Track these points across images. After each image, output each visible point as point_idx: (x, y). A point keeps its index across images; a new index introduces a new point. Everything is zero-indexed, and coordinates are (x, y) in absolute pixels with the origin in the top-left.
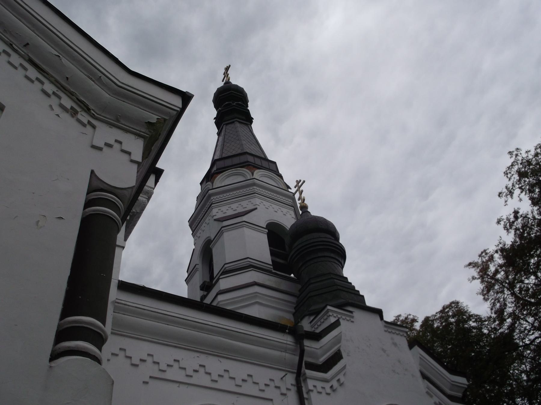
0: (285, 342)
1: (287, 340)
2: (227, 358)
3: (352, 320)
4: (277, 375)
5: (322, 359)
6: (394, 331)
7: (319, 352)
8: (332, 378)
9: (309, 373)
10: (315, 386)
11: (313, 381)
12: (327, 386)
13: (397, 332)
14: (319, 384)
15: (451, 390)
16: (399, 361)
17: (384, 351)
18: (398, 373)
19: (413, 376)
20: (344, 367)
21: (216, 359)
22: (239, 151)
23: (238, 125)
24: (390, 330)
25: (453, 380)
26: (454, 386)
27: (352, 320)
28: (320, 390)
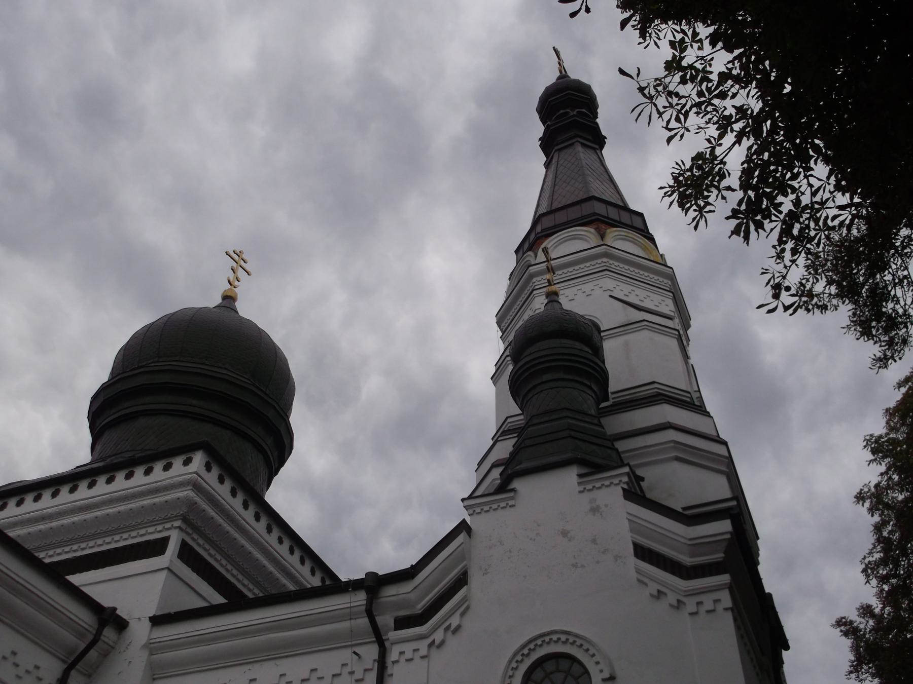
0: (349, 605)
1: (360, 598)
2: (287, 657)
3: (511, 503)
4: (346, 655)
5: (420, 607)
6: (598, 485)
7: (412, 596)
8: (434, 629)
9: (393, 635)
10: (402, 653)
11: (403, 646)
12: (423, 645)
13: (607, 483)
14: (408, 648)
15: (692, 555)
16: (594, 541)
17: (564, 533)
18: (583, 566)
19: (616, 558)
20: (465, 599)
21: (272, 663)
22: (582, 196)
23: (579, 148)
24: (589, 487)
25: (692, 536)
26: (696, 546)
27: (511, 503)
28: (409, 655)
